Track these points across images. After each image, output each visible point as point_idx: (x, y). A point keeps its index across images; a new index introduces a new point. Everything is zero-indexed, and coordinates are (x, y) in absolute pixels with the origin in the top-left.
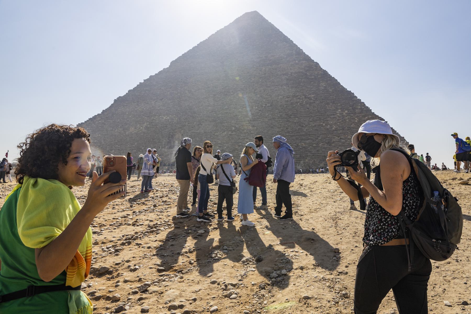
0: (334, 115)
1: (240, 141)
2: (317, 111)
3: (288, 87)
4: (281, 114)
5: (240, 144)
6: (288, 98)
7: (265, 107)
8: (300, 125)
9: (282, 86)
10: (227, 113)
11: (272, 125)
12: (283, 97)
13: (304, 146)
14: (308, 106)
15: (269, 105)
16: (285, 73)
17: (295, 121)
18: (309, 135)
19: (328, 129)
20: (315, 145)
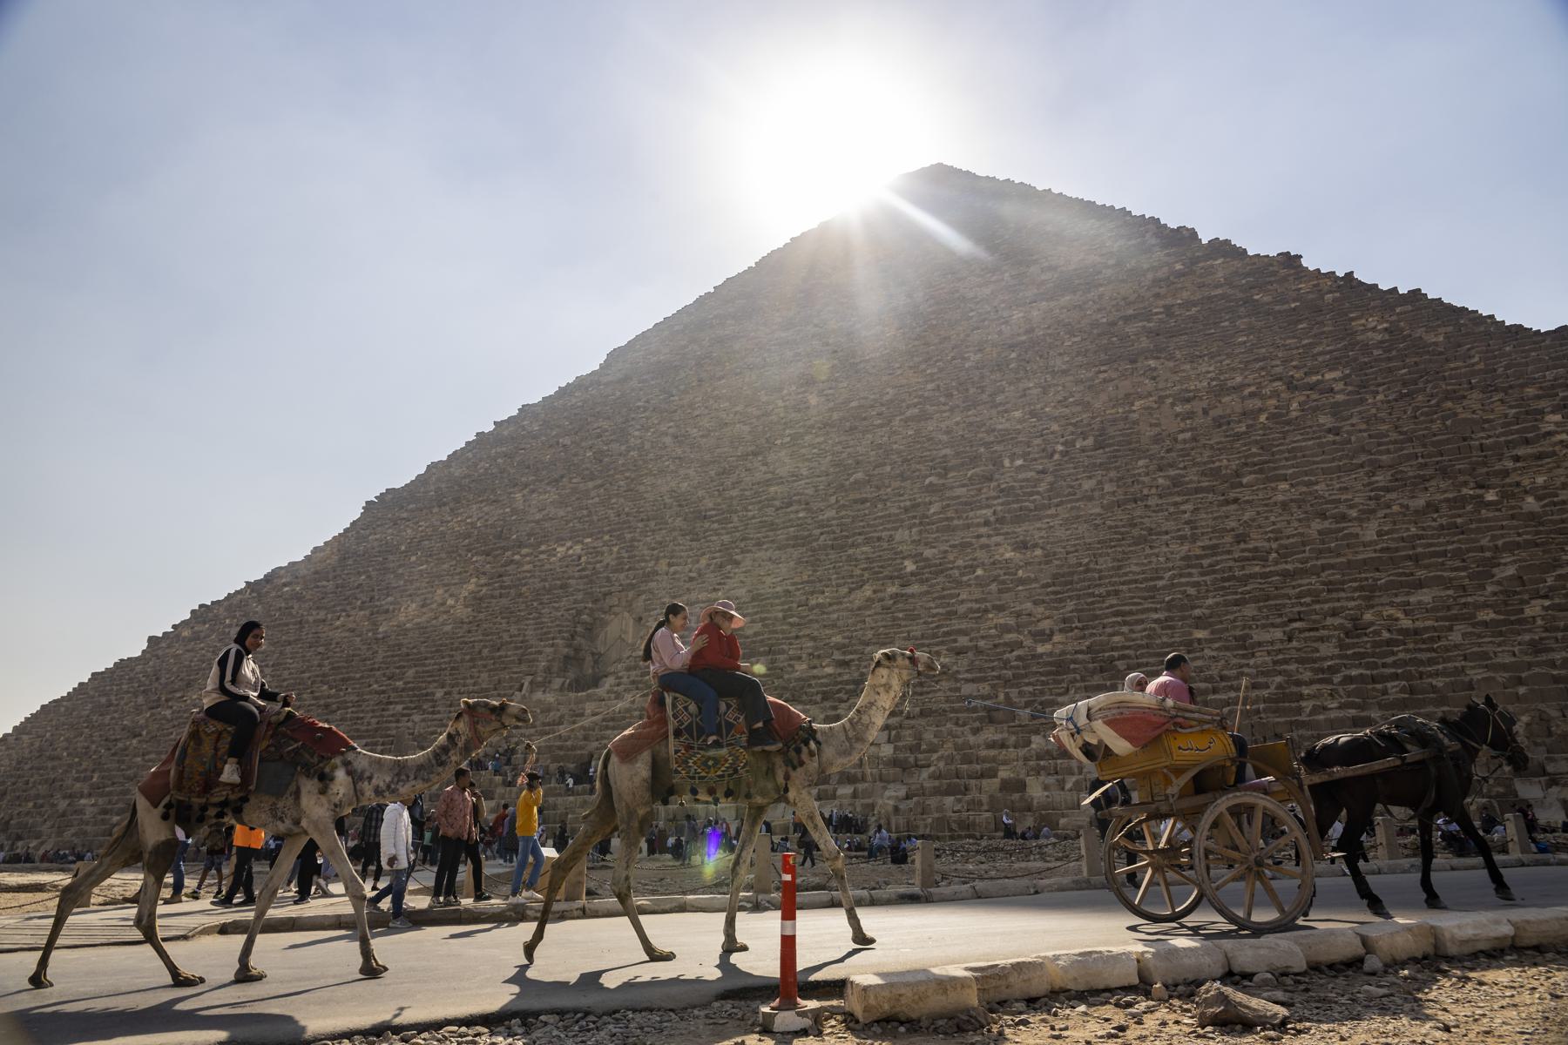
0: (1527, 442)
1: (956, 624)
2: (1394, 436)
3: (1171, 358)
4: (1172, 473)
5: (963, 641)
6: (1188, 400)
7: (1064, 454)
8: (1323, 516)
9: (1133, 362)
10: (864, 501)
11: (1136, 532)
12: (1161, 400)
13: (1406, 623)
14: (1325, 420)
15: (1090, 442)
16: (1131, 312)
17: (1280, 498)
18: (1416, 559)
19: (1532, 516)
20: (1487, 615)
